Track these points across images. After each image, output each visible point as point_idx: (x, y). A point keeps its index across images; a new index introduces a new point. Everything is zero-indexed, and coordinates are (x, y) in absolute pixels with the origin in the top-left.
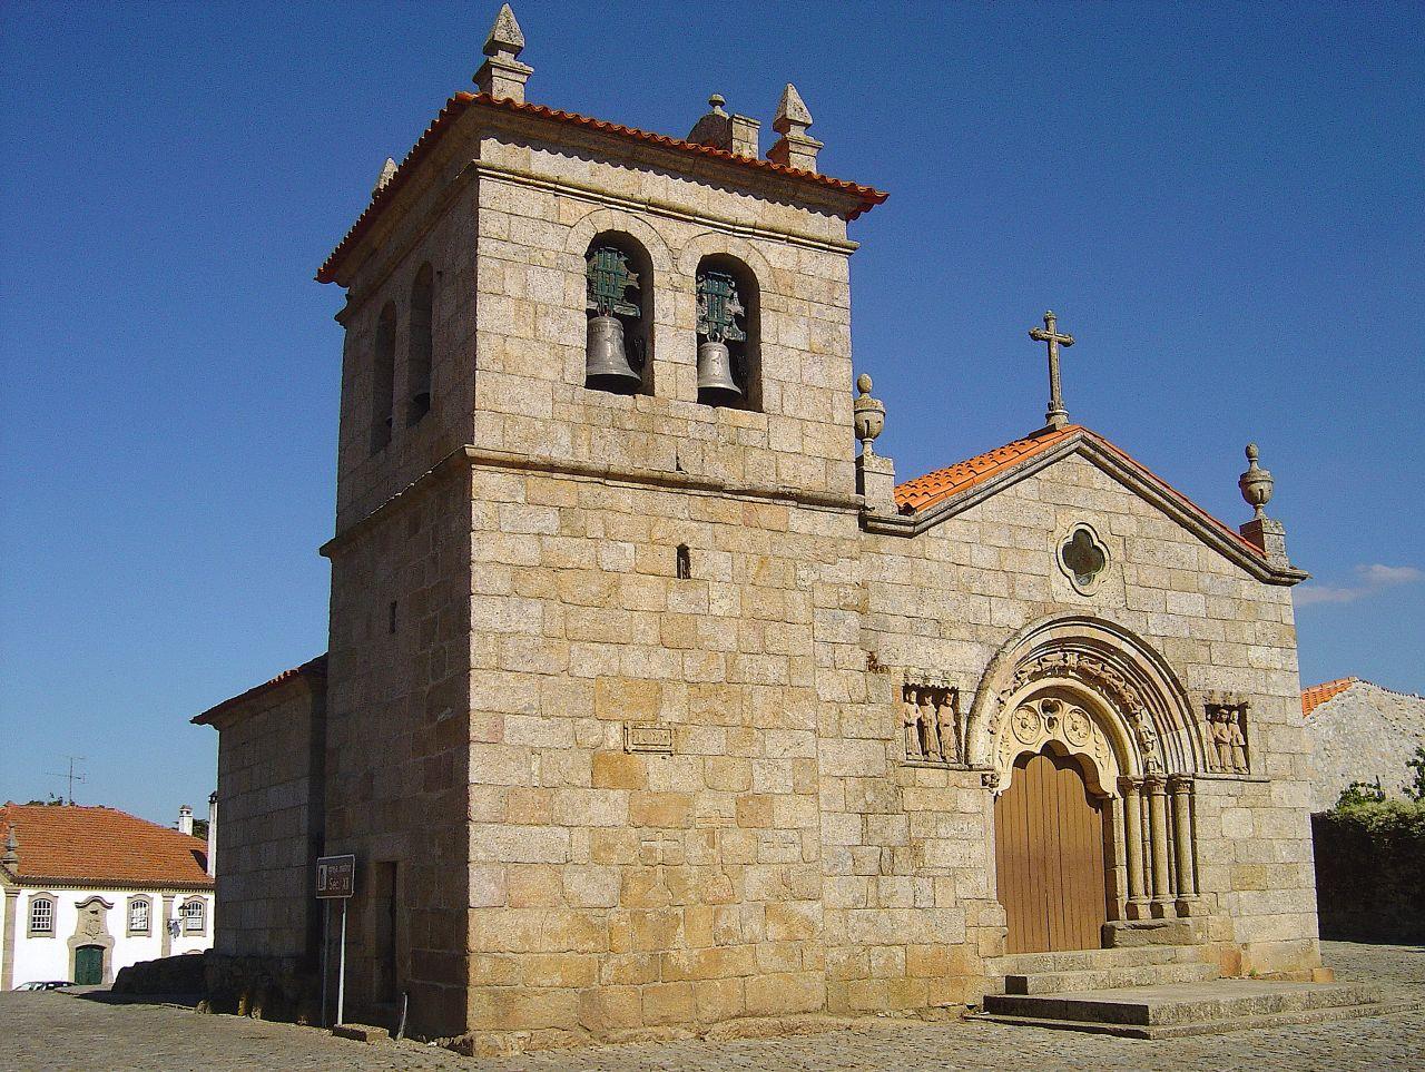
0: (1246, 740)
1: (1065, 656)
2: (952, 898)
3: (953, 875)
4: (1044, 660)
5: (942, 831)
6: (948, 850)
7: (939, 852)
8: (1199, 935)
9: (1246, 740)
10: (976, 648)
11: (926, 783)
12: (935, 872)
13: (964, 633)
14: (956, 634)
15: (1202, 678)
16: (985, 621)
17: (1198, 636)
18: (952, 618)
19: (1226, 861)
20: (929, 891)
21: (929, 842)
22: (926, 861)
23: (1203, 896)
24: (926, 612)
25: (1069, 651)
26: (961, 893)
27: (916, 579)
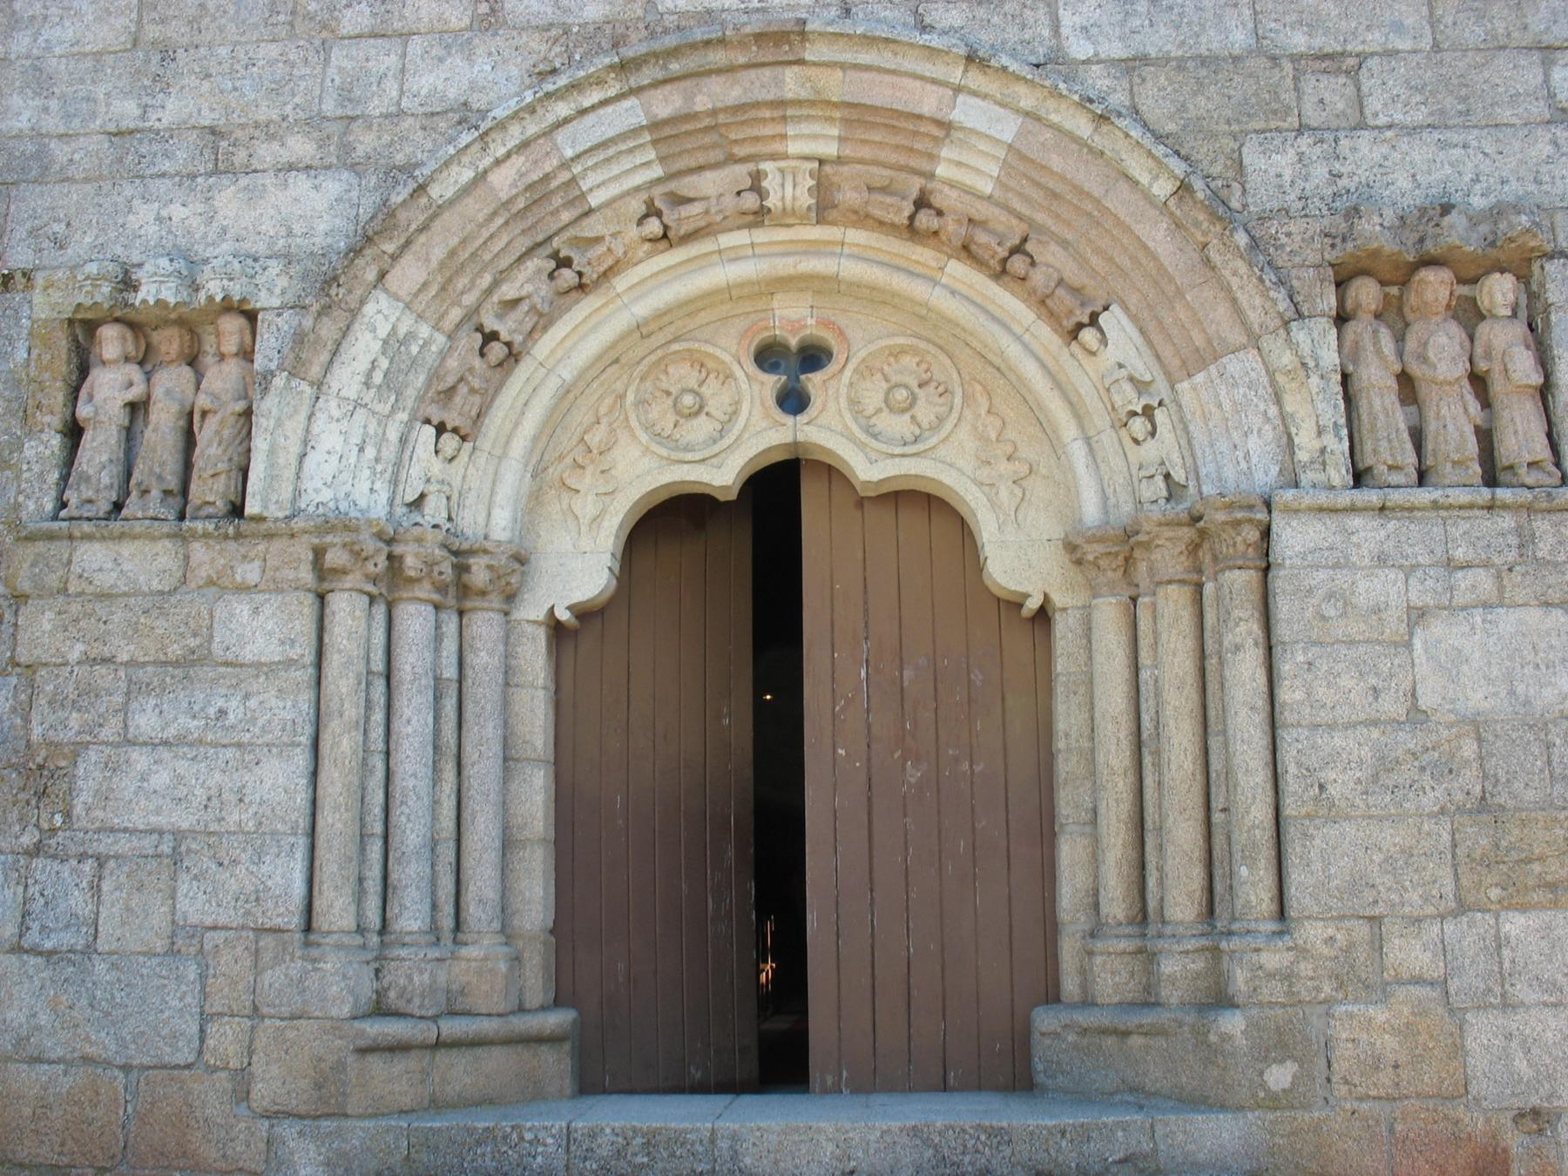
0: (1544, 361)
1: (757, 177)
2: (159, 916)
3: (174, 853)
4: (680, 200)
5: (145, 721)
6: (161, 779)
7: (126, 785)
8: (1279, 1076)
9: (1544, 361)
10: (333, 186)
11: (106, 580)
12: (105, 844)
13: (300, 147)
14: (267, 153)
15: (1320, 172)
16: (375, 107)
17: (1299, 41)
18: (265, 113)
19: (1429, 801)
20: (78, 901)
21: (93, 755)
22: (79, 810)
23: (1313, 933)
24: (171, 110)
25: (773, 157)
26: (194, 905)
27: (152, 32)
